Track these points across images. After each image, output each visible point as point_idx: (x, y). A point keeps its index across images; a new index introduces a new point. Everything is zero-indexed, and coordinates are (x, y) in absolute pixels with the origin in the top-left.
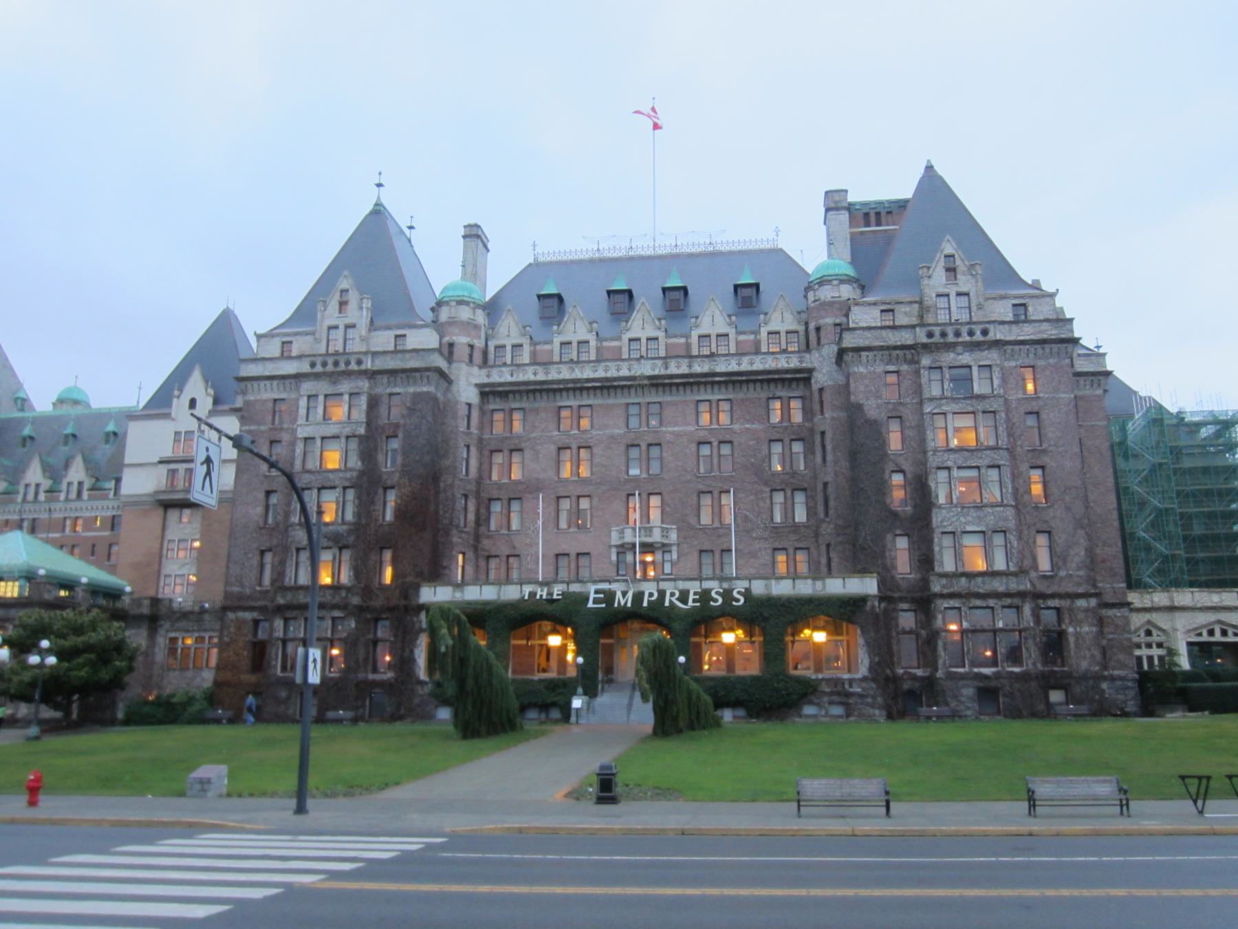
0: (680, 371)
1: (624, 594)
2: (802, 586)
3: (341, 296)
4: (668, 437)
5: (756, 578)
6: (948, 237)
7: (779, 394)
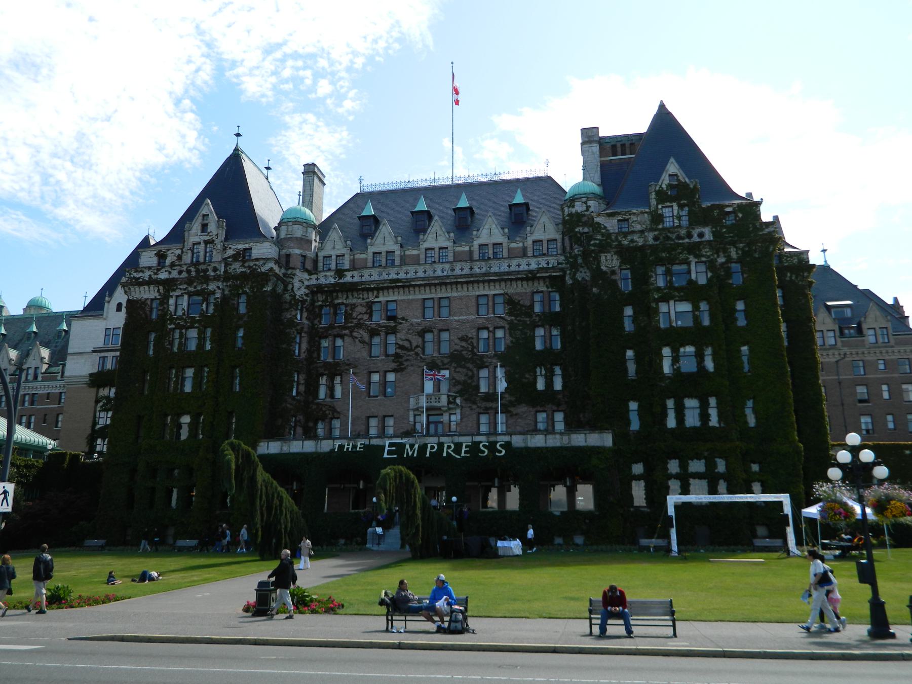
0: (464, 273)
1: (412, 446)
2: (551, 441)
3: (203, 220)
4: (455, 324)
5: (515, 434)
6: (672, 160)
7: (541, 289)
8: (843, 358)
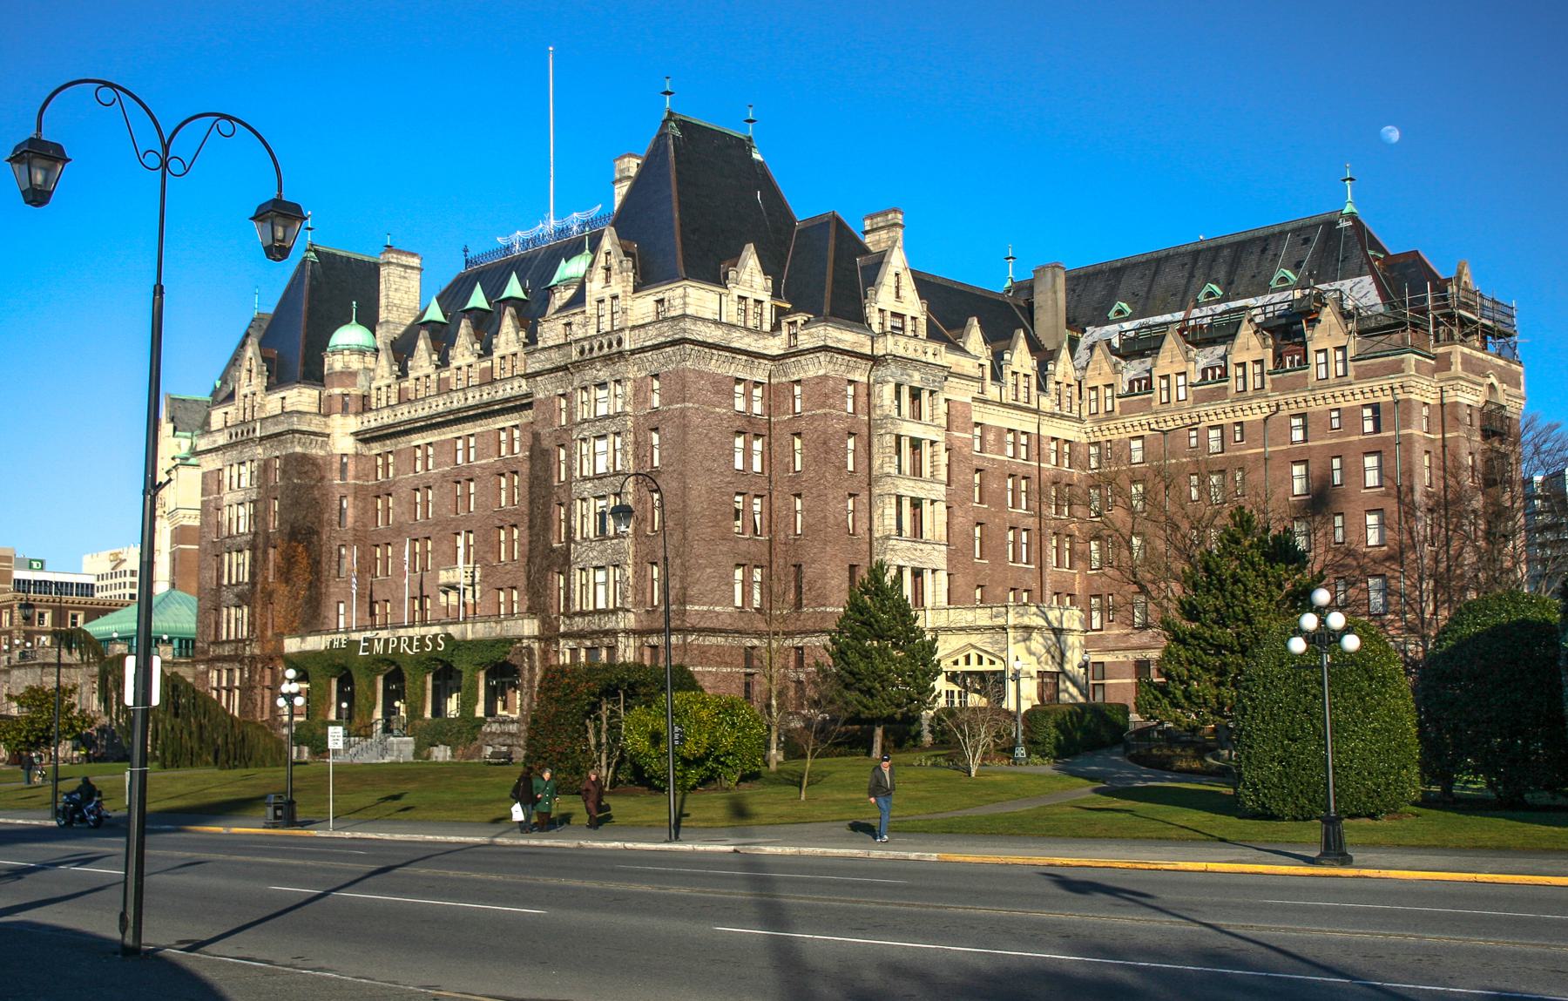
1: (379, 640)
4: (478, 471)
8: (1275, 413)
